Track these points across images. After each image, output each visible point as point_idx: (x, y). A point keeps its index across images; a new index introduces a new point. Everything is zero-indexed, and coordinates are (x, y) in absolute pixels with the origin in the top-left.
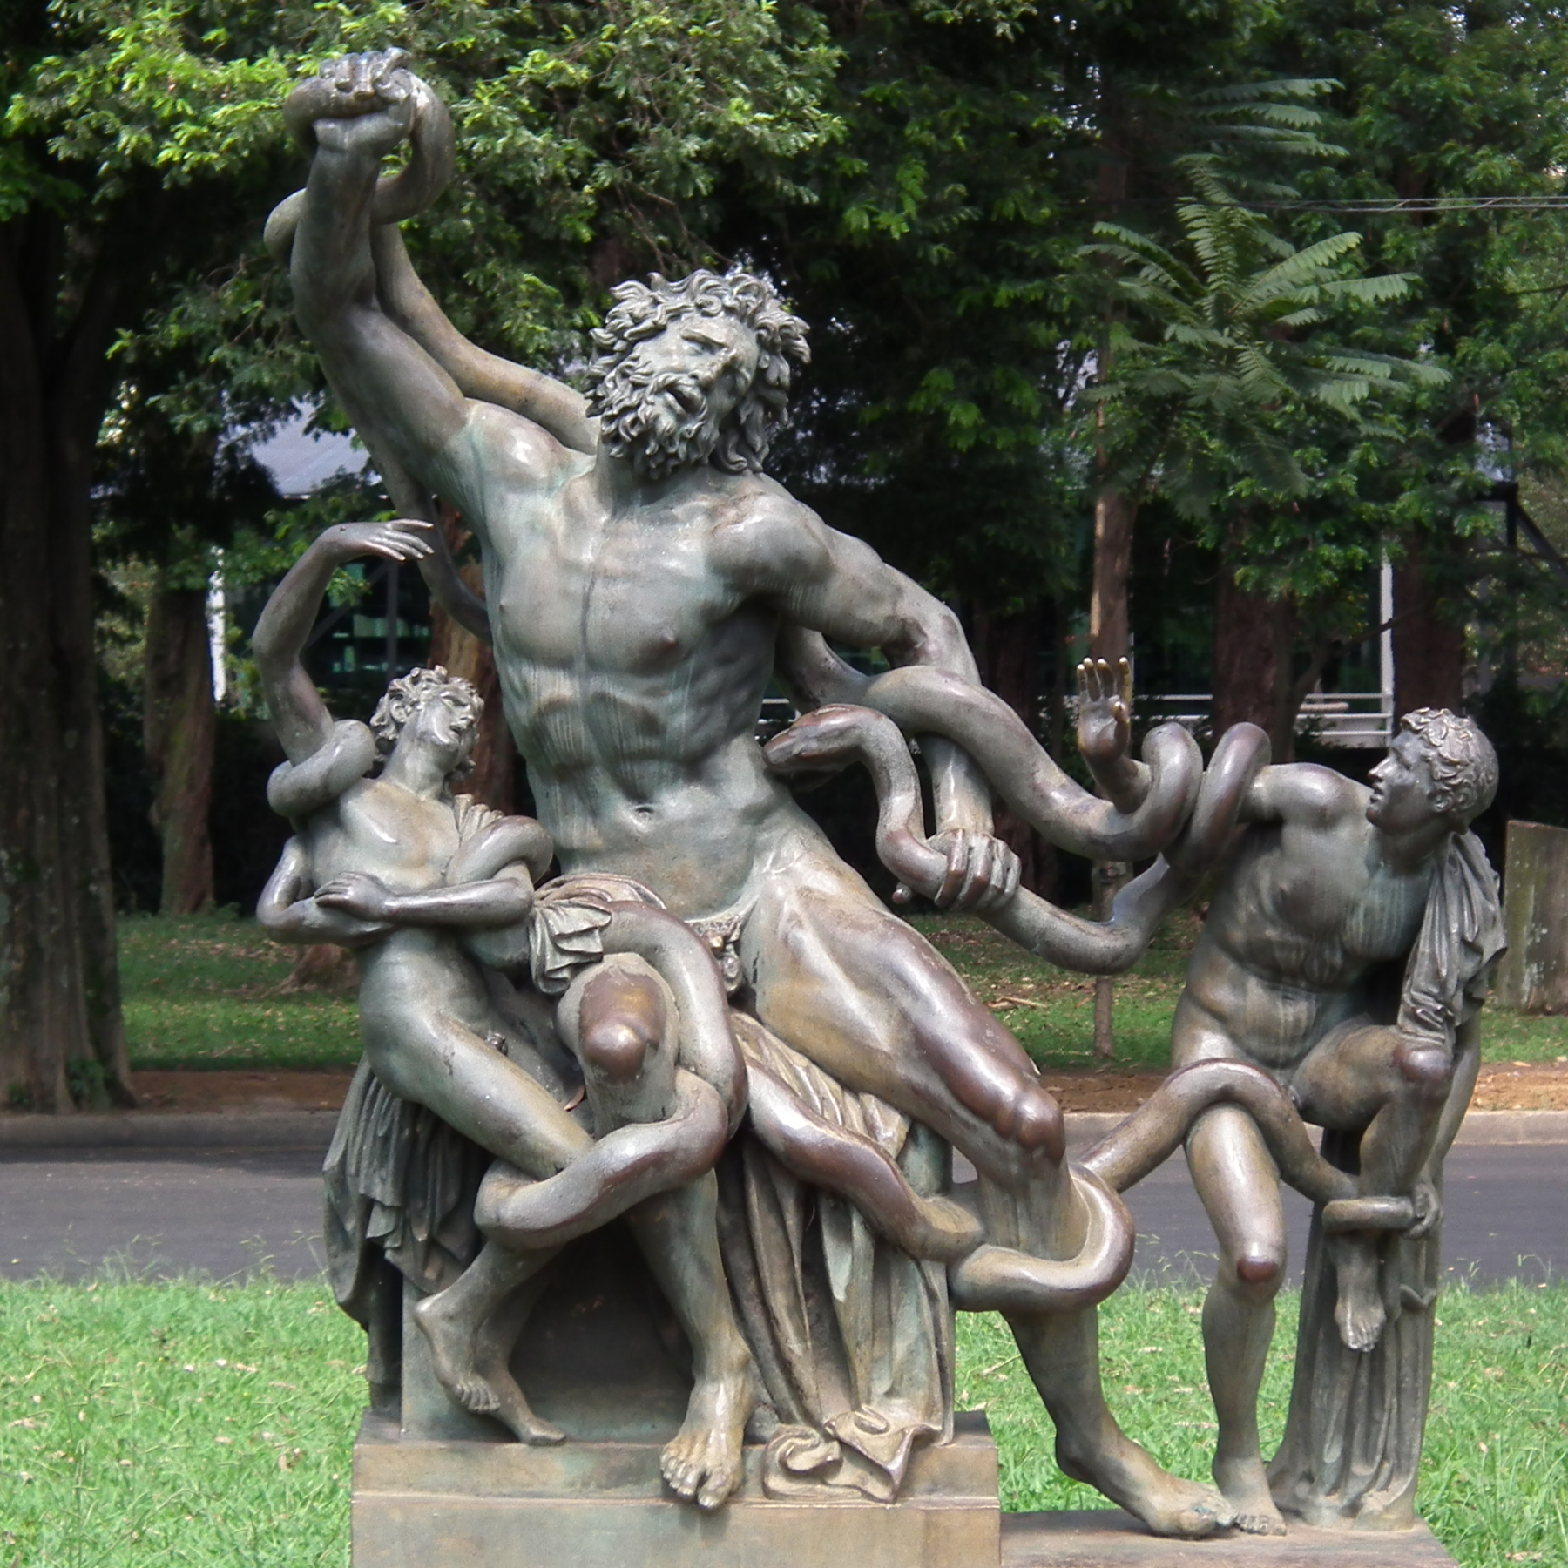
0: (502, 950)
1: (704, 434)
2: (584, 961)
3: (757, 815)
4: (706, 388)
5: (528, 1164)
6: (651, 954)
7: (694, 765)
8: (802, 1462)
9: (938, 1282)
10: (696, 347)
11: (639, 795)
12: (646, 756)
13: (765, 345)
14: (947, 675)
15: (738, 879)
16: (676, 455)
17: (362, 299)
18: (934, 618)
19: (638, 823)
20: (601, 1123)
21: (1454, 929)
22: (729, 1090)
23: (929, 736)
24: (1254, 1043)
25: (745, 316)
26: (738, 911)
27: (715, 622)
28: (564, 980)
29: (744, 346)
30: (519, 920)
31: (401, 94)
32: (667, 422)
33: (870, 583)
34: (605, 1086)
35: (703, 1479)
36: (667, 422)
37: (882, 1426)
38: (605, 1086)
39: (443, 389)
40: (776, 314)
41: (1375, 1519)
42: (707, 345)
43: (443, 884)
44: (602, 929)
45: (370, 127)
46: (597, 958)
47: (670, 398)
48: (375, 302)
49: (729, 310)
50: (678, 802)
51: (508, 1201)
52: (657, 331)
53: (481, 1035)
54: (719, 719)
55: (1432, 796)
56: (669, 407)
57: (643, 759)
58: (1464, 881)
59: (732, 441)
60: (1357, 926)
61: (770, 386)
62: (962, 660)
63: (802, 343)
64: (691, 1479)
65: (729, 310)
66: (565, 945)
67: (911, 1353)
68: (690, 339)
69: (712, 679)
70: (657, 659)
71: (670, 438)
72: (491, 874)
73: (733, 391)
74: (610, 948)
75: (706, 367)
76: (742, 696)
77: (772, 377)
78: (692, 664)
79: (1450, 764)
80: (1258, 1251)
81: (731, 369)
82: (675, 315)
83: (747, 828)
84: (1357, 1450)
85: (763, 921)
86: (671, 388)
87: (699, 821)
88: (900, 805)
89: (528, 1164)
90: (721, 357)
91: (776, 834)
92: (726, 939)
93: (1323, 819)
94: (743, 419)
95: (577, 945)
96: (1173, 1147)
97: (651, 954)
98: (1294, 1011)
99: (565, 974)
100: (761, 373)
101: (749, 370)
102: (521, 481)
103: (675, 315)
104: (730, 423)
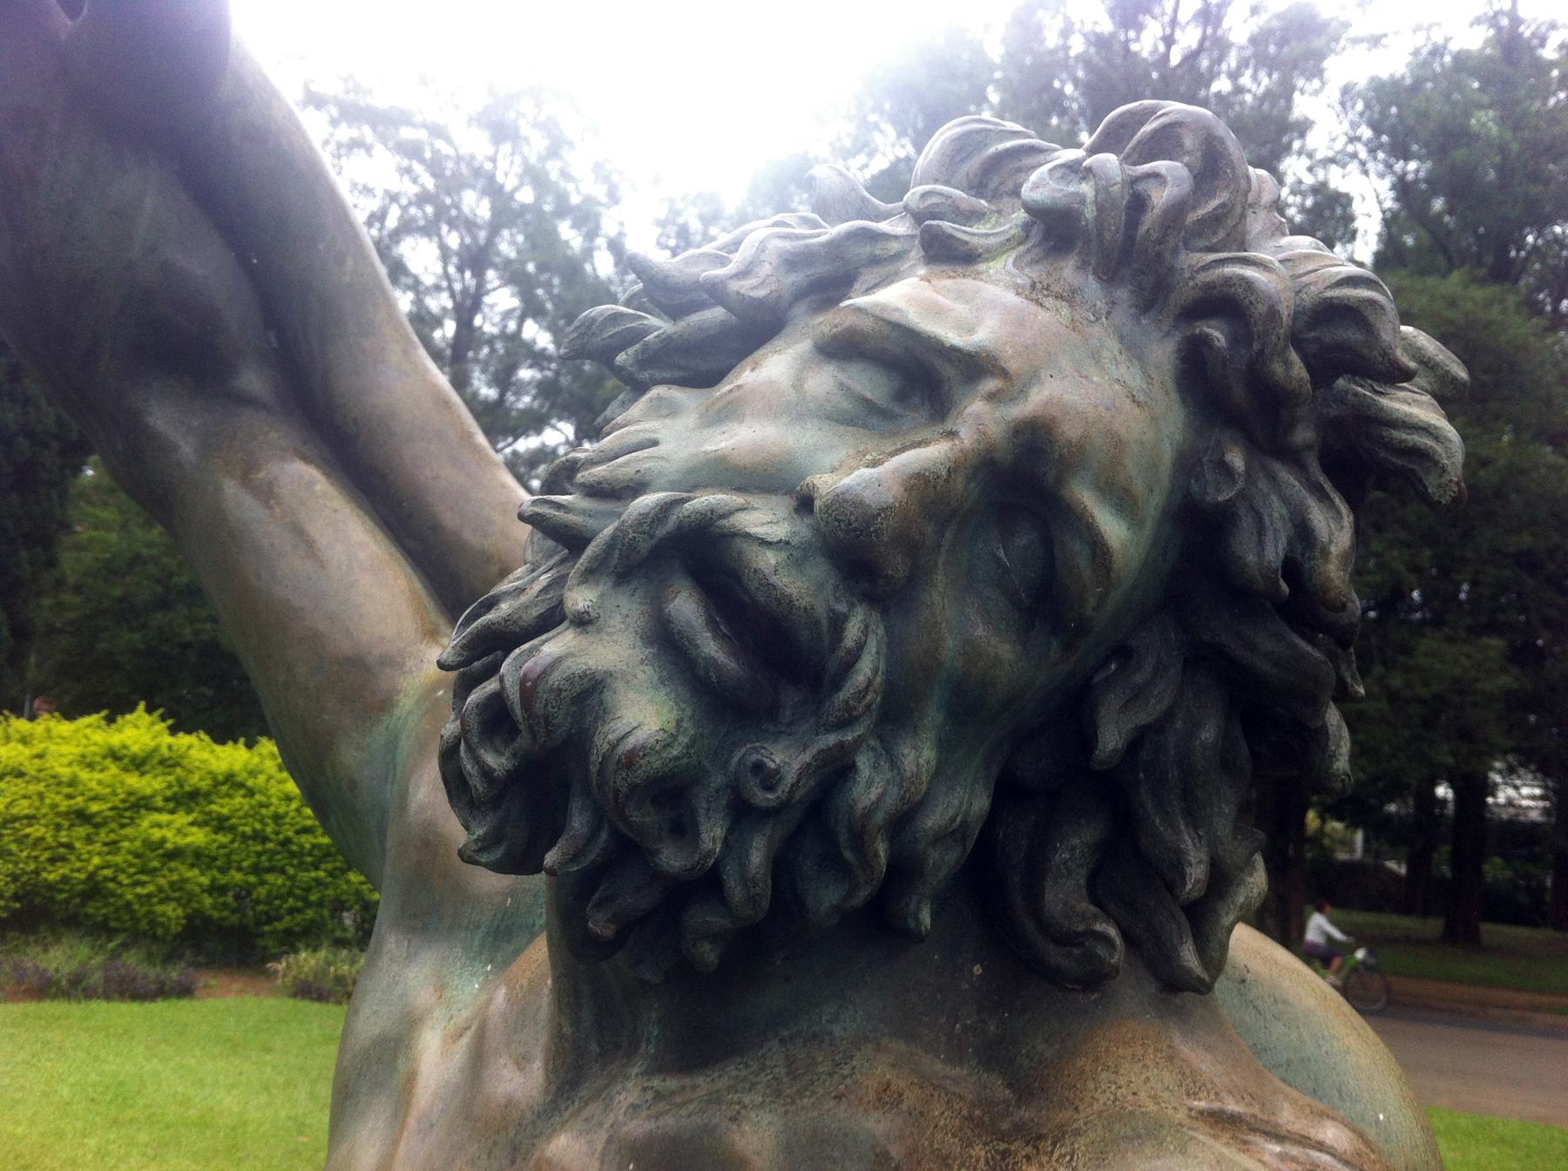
1: (871, 788)
4: (855, 549)
10: (868, 383)
16: (708, 883)
32: (644, 716)
36: (644, 716)
42: (919, 376)
47: (685, 606)
48: (253, 380)
56: (667, 643)
59: (1074, 848)
61: (1241, 596)
71: (671, 791)
73: (1044, 603)
90: (979, 420)
94: (1111, 738)
100: (1198, 532)
101: (1124, 503)
104: (1048, 765)
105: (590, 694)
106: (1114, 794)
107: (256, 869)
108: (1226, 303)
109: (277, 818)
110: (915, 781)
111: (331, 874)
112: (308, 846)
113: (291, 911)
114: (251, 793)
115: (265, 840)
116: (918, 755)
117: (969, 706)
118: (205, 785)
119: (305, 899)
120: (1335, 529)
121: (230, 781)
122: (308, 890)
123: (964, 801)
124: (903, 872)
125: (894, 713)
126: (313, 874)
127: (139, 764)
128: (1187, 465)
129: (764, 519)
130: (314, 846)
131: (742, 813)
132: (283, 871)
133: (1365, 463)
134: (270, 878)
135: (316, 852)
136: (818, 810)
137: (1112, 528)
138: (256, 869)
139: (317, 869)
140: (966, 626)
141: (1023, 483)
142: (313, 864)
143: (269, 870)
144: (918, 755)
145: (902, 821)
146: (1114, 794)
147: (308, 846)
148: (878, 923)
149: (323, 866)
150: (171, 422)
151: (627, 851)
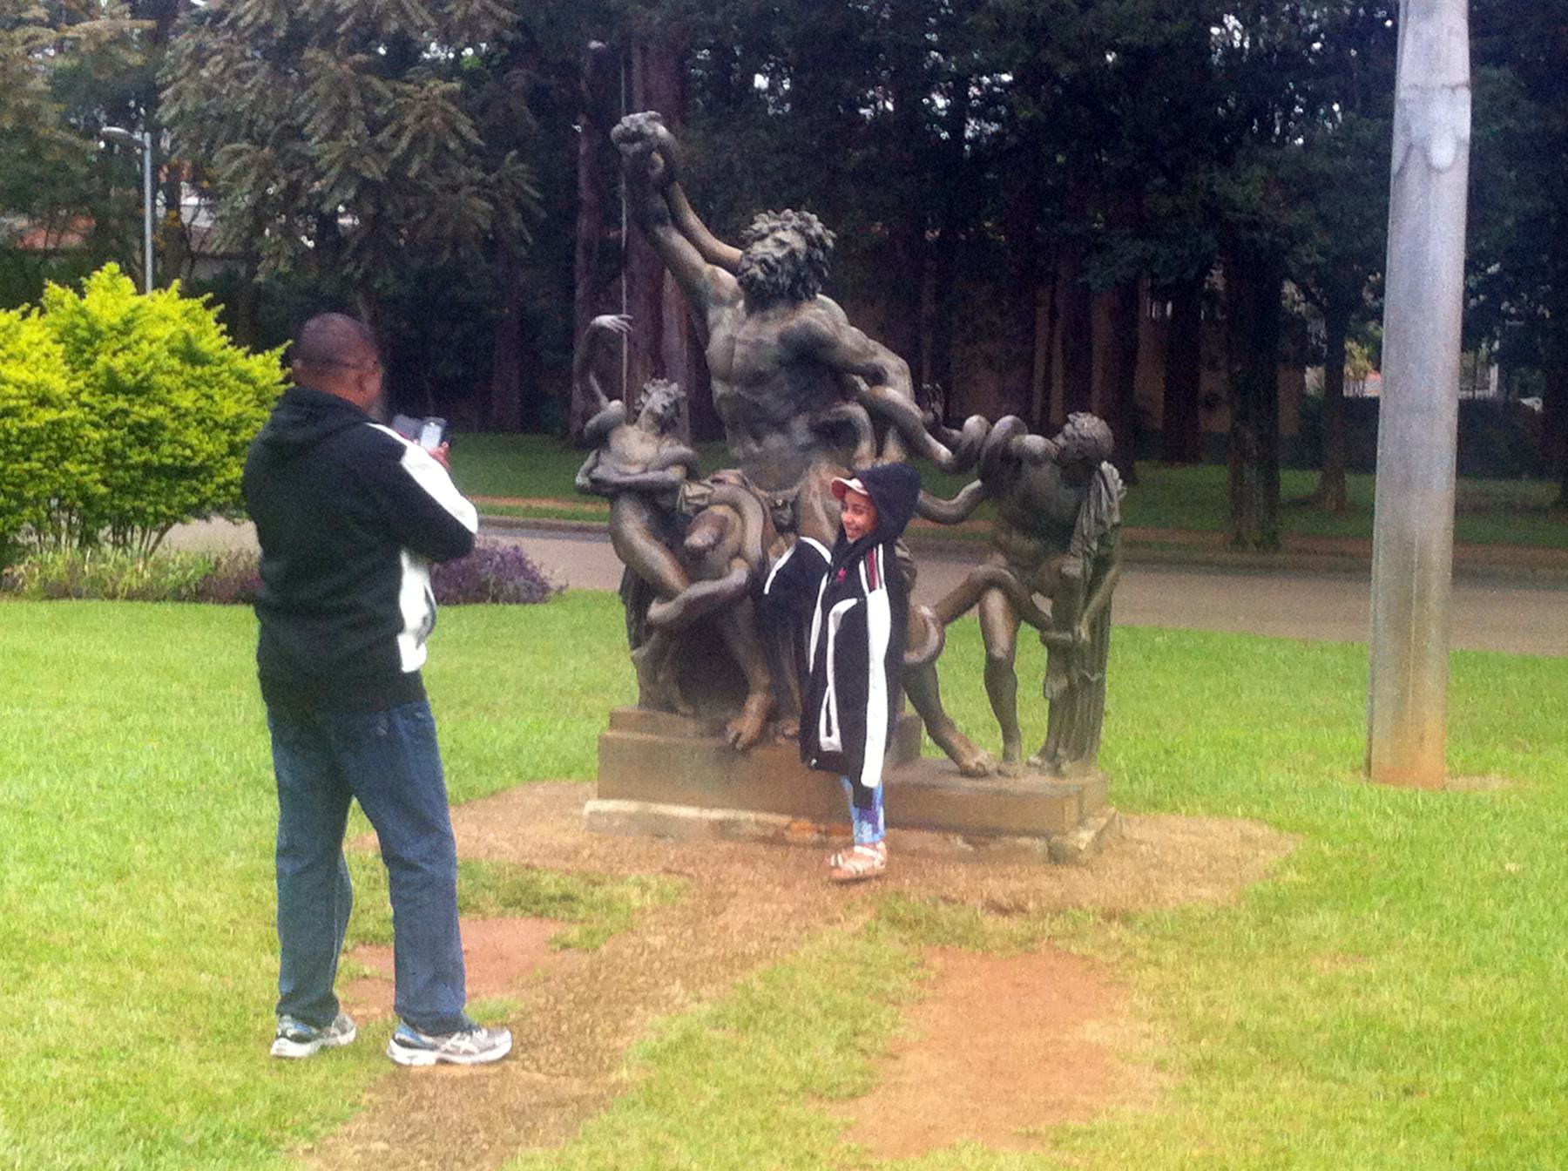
0: (665, 502)
2: (699, 509)
3: (806, 448)
4: (778, 261)
5: (667, 594)
6: (736, 507)
7: (781, 426)
11: (758, 438)
12: (760, 421)
14: (898, 392)
15: (796, 477)
17: (661, 221)
18: (891, 362)
19: (756, 450)
20: (693, 577)
22: (756, 567)
23: (884, 418)
25: (800, 231)
26: (796, 490)
29: (798, 243)
30: (672, 489)
31: (650, 131)
32: (761, 276)
33: (857, 348)
34: (695, 564)
35: (739, 735)
36: (761, 276)
38: (695, 564)
39: (696, 258)
40: (818, 228)
41: (1063, 776)
42: (781, 244)
43: (645, 471)
45: (638, 146)
46: (704, 508)
49: (794, 228)
50: (774, 441)
51: (656, 610)
52: (763, 237)
53: (657, 539)
54: (792, 405)
57: (756, 423)
60: (1053, 509)
62: (905, 382)
63: (830, 243)
64: (733, 735)
65: (794, 228)
68: (776, 240)
70: (756, 379)
72: (664, 468)
74: (711, 504)
75: (780, 254)
80: (998, 654)
81: (792, 253)
82: (773, 230)
85: (803, 496)
86: (764, 261)
88: (865, 447)
89: (667, 594)
92: (785, 503)
93: (1036, 460)
95: (697, 502)
96: (972, 605)
97: (736, 507)
98: (1031, 545)
100: (809, 256)
102: (720, 301)
103: (773, 230)
104: (797, 279)
106: (804, 281)
110: (785, 281)
111: (45, 464)
112: (15, 432)
119: (18, 497)
120: (821, 254)
122: (21, 485)
123: (789, 282)
126: (26, 466)
129: (770, 260)
130: (22, 431)
133: (824, 247)
135: (25, 438)
139: (28, 459)
140: (788, 266)
141: (792, 253)
142: (22, 454)
146: (804, 281)
147: (15, 432)
148: (781, 295)
149: (35, 455)
150: (660, 232)
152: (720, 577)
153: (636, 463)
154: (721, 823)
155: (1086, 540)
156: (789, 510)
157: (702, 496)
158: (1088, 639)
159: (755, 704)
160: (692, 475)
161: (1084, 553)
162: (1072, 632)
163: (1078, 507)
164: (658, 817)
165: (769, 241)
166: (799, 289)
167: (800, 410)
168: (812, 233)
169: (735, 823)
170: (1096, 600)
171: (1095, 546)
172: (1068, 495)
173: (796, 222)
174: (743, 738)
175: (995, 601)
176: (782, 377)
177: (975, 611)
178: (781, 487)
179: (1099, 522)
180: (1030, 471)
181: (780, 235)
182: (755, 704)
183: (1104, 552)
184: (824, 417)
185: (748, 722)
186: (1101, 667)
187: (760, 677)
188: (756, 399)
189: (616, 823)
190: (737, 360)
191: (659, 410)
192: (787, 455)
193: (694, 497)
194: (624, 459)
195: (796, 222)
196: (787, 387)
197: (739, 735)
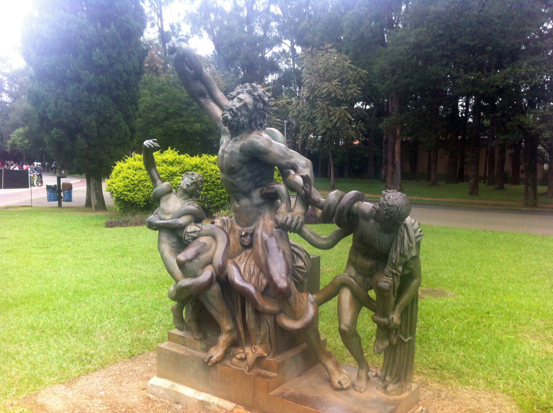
1: (241, 120)
2: (194, 238)
3: (259, 206)
6: (214, 237)
7: (247, 194)
8: (238, 356)
9: (270, 320)
13: (255, 99)
15: (255, 220)
16: (234, 125)
17: (203, 95)
21: (398, 249)
22: (217, 270)
24: (359, 270)
26: (252, 228)
27: (243, 163)
28: (190, 242)
30: (182, 227)
32: (230, 117)
36: (230, 117)
37: (254, 351)
42: (241, 100)
44: (198, 231)
47: (231, 112)
48: (208, 96)
49: (247, 92)
50: (245, 202)
55: (386, 214)
56: (230, 114)
58: (404, 237)
61: (258, 109)
65: (247, 92)
66: (189, 234)
67: (265, 335)
69: (248, 175)
71: (231, 121)
76: (258, 179)
77: (258, 107)
78: (241, 172)
79: (389, 206)
83: (256, 209)
84: (388, 373)
86: (231, 110)
87: (246, 206)
90: (243, 102)
91: (263, 211)
93: (366, 217)
95: (194, 235)
97: (214, 237)
99: (190, 241)
100: (255, 106)
105: (227, 117)
107: (206, 190)
108: (254, 95)
109: (210, 176)
113: (217, 201)
114: (202, 169)
115: (208, 182)
116: (243, 118)
117: (245, 116)
118: (190, 168)
119: (220, 198)
121: (196, 167)
122: (221, 195)
124: (244, 124)
125: (241, 116)
127: (171, 164)
128: (254, 103)
129: (234, 108)
131: (235, 122)
132: (214, 190)
134: (210, 192)
136: (238, 121)
137: (250, 107)
138: (206, 190)
140: (244, 112)
141: (245, 105)
143: (210, 190)
144: (243, 118)
145: (243, 121)
150: (202, 100)
151: (230, 124)
152: (196, 276)
153: (169, 214)
154: (202, 401)
155: (394, 266)
156: (248, 238)
157: (195, 232)
158: (398, 322)
159: (223, 339)
160: (197, 220)
161: (393, 274)
162: (388, 317)
163: (391, 245)
164: (177, 393)
165: (235, 100)
166: (253, 125)
167: (257, 186)
168: (256, 94)
169: (208, 404)
170: (405, 298)
171: (400, 269)
172: (385, 238)
173: (249, 88)
174: (212, 359)
175: (346, 295)
176: (245, 170)
177: (336, 298)
178: (248, 225)
179: (402, 255)
180: (362, 222)
181: (241, 96)
182: (223, 339)
183: (407, 272)
184: (266, 190)
185: (216, 353)
186: (412, 332)
187: (227, 326)
188: (233, 181)
189: (161, 392)
190: (224, 161)
191: (185, 187)
192: (250, 209)
193: (191, 232)
194: (163, 211)
195: (249, 88)
196: (248, 175)
197: (211, 357)
